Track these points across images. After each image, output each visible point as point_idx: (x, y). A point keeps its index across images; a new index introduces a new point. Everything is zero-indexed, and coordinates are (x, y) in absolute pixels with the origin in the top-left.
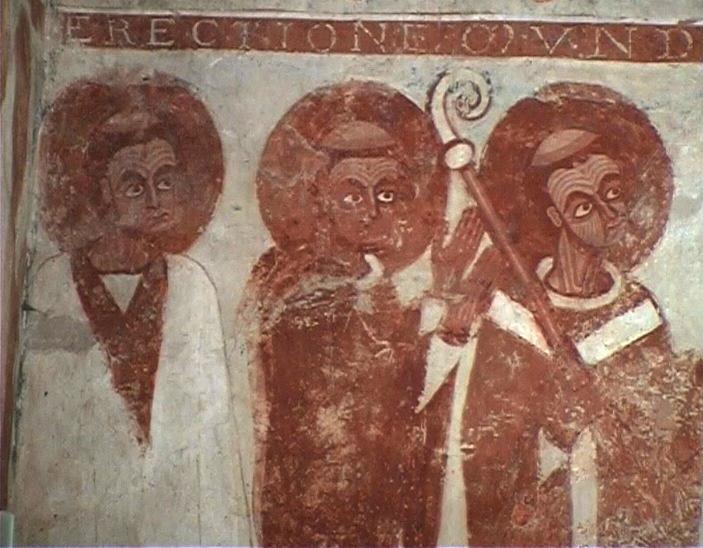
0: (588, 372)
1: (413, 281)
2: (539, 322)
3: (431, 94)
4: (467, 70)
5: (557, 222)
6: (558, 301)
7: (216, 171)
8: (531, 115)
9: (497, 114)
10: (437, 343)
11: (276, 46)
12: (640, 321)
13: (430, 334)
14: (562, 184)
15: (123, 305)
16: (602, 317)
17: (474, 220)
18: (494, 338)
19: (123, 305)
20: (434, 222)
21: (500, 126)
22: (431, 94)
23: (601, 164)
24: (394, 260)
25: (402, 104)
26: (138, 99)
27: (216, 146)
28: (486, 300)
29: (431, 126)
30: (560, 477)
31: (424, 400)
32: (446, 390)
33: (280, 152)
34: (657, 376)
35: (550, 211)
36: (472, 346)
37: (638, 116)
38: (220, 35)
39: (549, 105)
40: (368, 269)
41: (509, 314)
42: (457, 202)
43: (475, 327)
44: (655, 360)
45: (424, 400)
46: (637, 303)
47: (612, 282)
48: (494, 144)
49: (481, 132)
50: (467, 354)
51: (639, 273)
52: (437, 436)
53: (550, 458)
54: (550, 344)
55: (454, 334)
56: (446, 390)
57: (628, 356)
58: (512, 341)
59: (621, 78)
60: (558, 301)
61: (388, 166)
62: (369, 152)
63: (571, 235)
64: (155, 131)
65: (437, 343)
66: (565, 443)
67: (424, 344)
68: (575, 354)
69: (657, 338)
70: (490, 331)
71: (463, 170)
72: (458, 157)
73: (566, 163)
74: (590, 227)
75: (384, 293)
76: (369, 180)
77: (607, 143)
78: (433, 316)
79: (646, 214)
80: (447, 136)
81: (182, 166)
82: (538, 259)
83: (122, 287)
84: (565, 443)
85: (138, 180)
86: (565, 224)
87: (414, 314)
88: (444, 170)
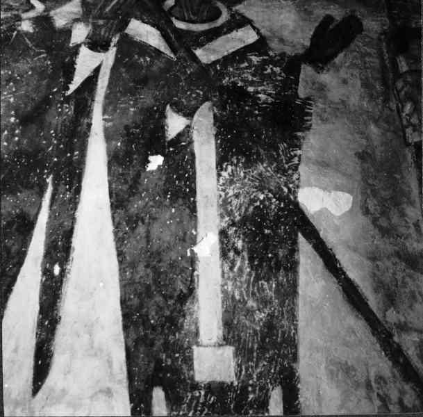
2: (165, 36)
6: (180, 25)
10: (84, 51)
13: (78, 46)
18: (130, 48)
30: (185, 134)
31: (73, 87)
32: (91, 82)
36: (113, 51)
43: (115, 40)
45: (73, 87)
47: (219, 14)
50: (108, 58)
51: (239, 8)
53: (175, 124)
54: (174, 51)
55: (97, 44)
56: (91, 82)
58: (144, 48)
60: (180, 25)
65: (84, 51)
66: (189, 114)
67: (75, 51)
68: (195, 59)
69: (261, 45)
75: (44, 21)
78: (80, 33)
87: (67, 32)
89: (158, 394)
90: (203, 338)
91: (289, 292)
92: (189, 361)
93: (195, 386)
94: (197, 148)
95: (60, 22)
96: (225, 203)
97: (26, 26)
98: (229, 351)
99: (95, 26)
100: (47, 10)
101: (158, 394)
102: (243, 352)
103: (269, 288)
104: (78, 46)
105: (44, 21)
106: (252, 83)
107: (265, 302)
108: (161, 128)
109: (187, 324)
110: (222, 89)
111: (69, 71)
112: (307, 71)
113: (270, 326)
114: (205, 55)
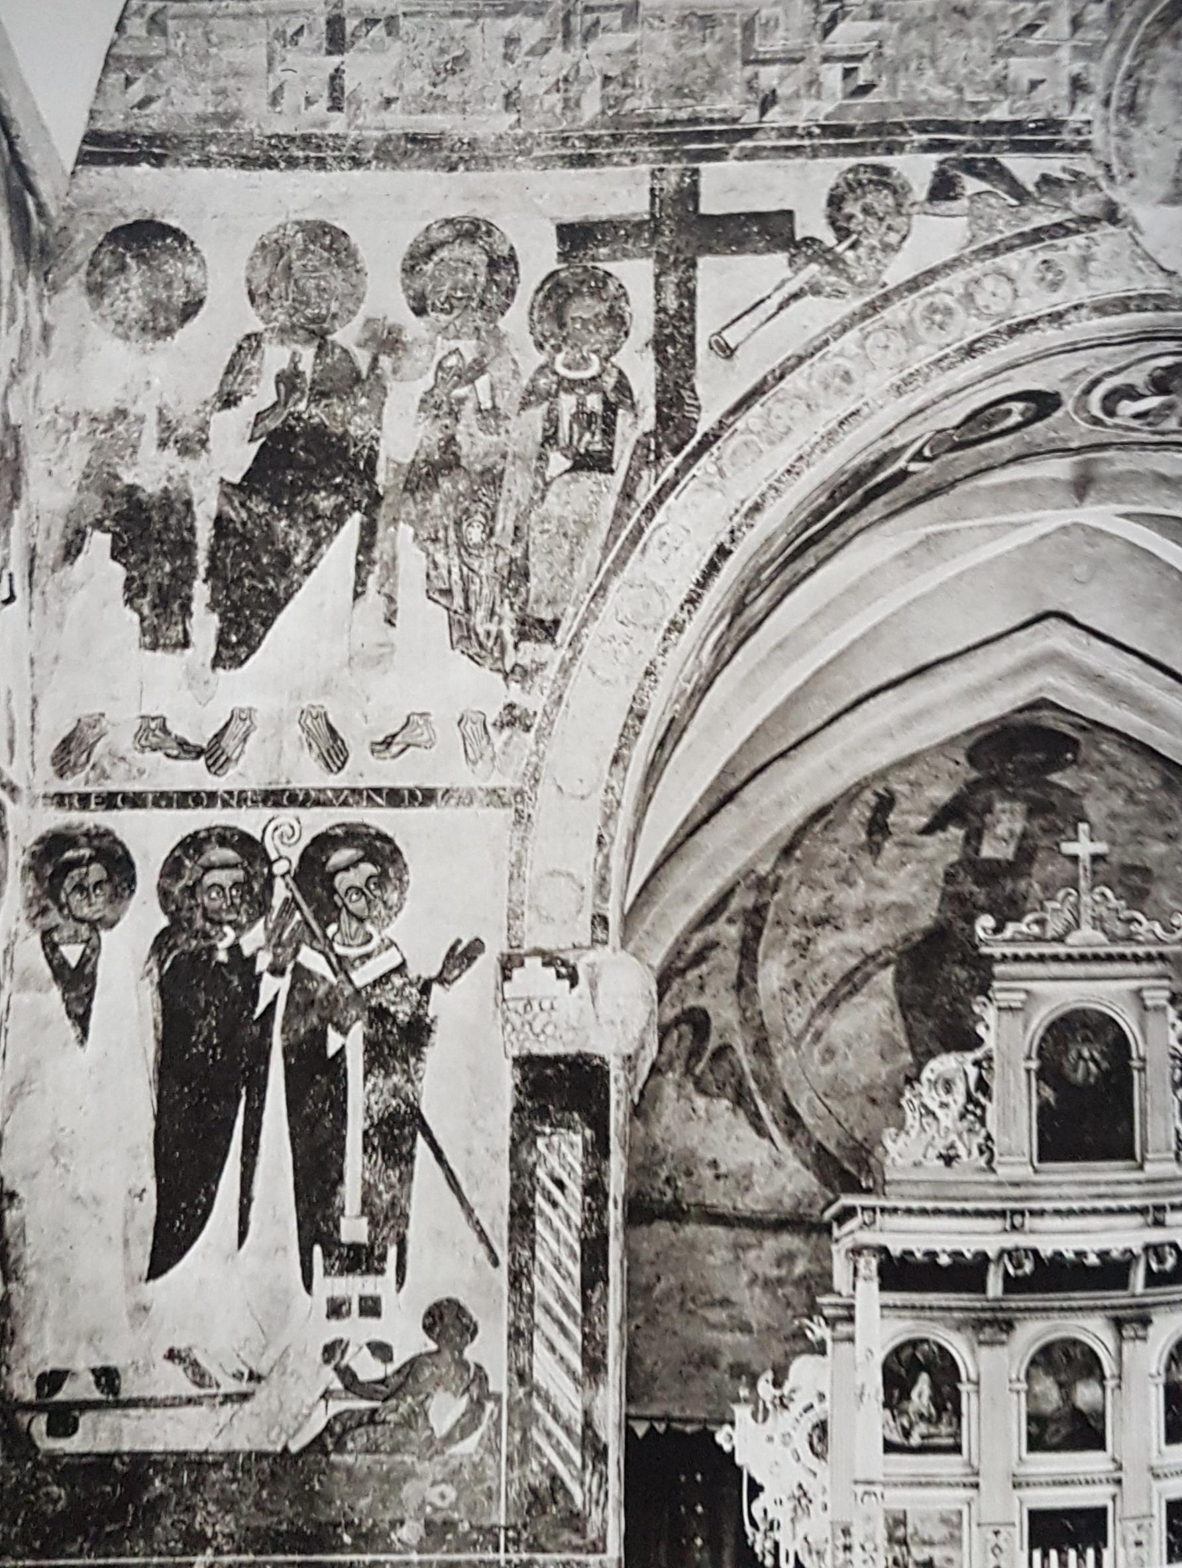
0: (358, 992)
1: (253, 940)
3: (264, 831)
4: (287, 815)
5: (340, 903)
7: (131, 881)
8: (324, 843)
9: (306, 840)
10: (267, 977)
11: (169, 806)
12: (389, 960)
14: (342, 881)
15: (73, 963)
16: (368, 956)
17: (290, 905)
18: (301, 973)
19: (73, 963)
20: (262, 906)
21: (306, 849)
22: (264, 831)
23: (368, 869)
24: (238, 927)
25: (246, 839)
26: (83, 840)
27: (131, 865)
28: (297, 951)
29: (265, 851)
31: (259, 1010)
32: (272, 1006)
33: (172, 868)
34: (400, 992)
35: (336, 898)
36: (288, 977)
37: (387, 840)
38: (135, 801)
39: (336, 836)
40: (225, 935)
41: (311, 958)
42: (280, 892)
43: (290, 967)
44: (397, 981)
45: (259, 1010)
46: (387, 948)
48: (303, 857)
49: (295, 854)
50: (285, 983)
51: (389, 932)
52: (267, 1032)
53: (334, 1041)
54: (336, 974)
55: (276, 970)
56: (272, 1006)
57: (384, 979)
58: (310, 975)
59: (379, 818)
60: (340, 950)
61: (239, 874)
62: (225, 866)
63: (348, 912)
64: (91, 860)
65: (267, 977)
66: (344, 1032)
68: (351, 981)
69: (400, 969)
70: (298, 967)
71: (283, 876)
72: (279, 868)
73: (346, 869)
74: (357, 905)
75: (234, 949)
76: (227, 884)
77: (369, 857)
78: (263, 962)
79: (393, 897)
80: (273, 856)
81: (110, 879)
82: (327, 925)
83: (72, 953)
84: (344, 1032)
85: (80, 887)
86: (345, 905)
87: (253, 959)
88: (272, 876)
89: (317, 1250)
90: (347, 1212)
91: (406, 1179)
92: (337, 1228)
93: (341, 1245)
94: (349, 1064)
95: (247, 951)
96: (368, 1108)
97: (222, 956)
98: (365, 1220)
99: (275, 955)
100: (237, 938)
101: (317, 1250)
102: (374, 1223)
103: (394, 1175)
104: (261, 974)
105: (234, 949)
106: (394, 1003)
107: (391, 1187)
108: (324, 1046)
109: (337, 1201)
110: (371, 1009)
111: (255, 996)
112: (436, 988)
113: (393, 1204)
114: (362, 976)
